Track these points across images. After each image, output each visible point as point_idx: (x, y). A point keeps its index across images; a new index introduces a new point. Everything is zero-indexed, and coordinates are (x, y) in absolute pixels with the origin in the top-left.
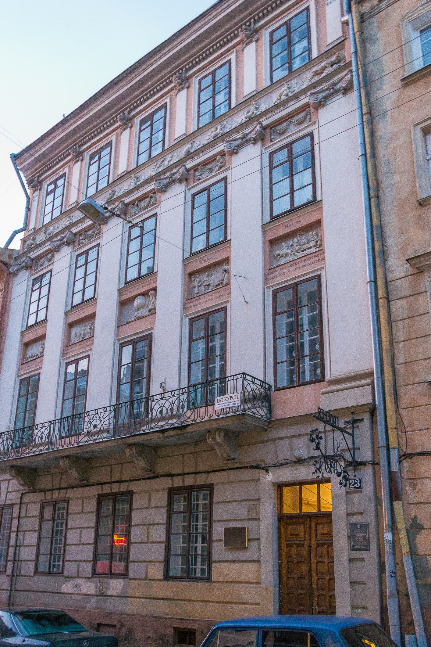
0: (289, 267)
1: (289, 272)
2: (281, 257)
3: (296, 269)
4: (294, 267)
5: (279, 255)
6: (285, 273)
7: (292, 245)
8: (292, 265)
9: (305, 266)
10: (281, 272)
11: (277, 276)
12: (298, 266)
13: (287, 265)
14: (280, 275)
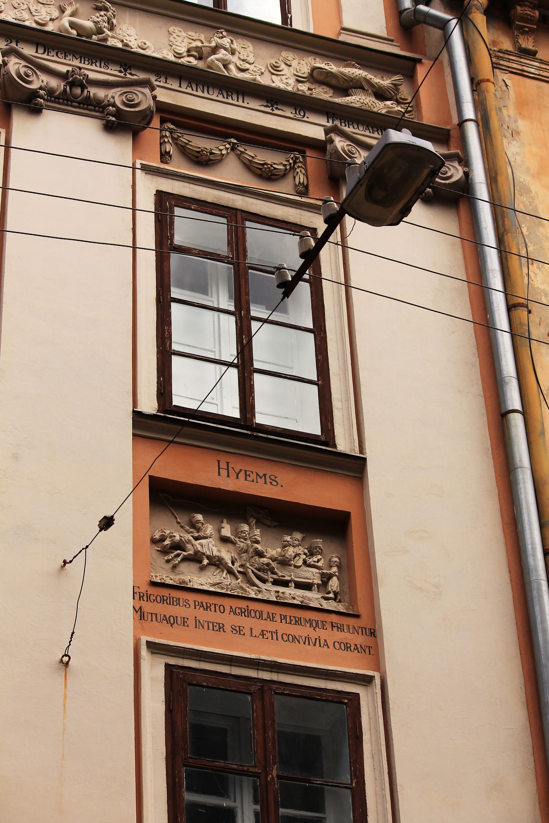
0: (233, 611)
1: (238, 630)
2: (186, 559)
3: (263, 634)
4: (258, 625)
5: (178, 546)
6: (221, 628)
7: (225, 540)
8: (246, 613)
9: (294, 638)
10: (204, 615)
11: (184, 621)
12: (270, 626)
13: (228, 603)
14: (198, 624)
